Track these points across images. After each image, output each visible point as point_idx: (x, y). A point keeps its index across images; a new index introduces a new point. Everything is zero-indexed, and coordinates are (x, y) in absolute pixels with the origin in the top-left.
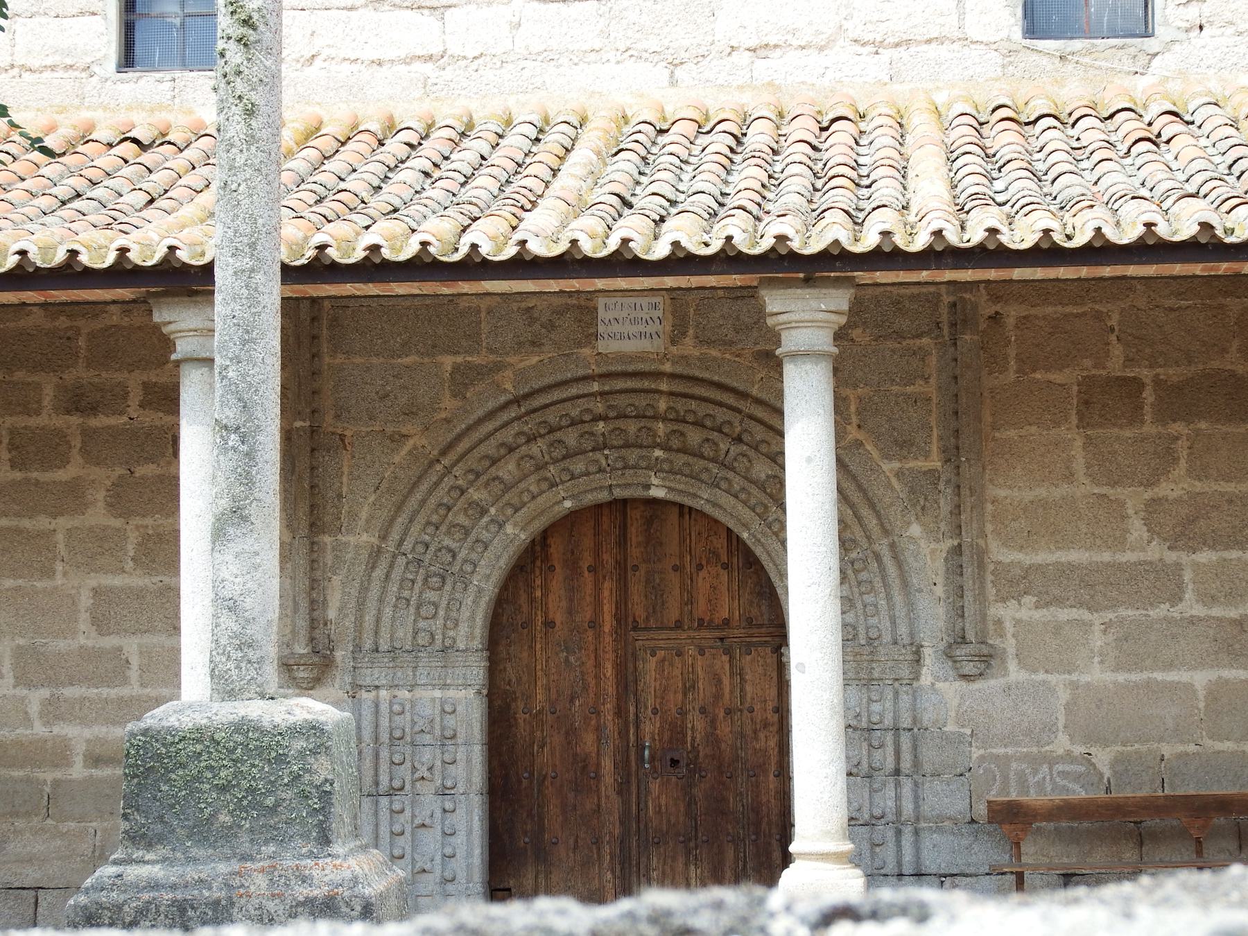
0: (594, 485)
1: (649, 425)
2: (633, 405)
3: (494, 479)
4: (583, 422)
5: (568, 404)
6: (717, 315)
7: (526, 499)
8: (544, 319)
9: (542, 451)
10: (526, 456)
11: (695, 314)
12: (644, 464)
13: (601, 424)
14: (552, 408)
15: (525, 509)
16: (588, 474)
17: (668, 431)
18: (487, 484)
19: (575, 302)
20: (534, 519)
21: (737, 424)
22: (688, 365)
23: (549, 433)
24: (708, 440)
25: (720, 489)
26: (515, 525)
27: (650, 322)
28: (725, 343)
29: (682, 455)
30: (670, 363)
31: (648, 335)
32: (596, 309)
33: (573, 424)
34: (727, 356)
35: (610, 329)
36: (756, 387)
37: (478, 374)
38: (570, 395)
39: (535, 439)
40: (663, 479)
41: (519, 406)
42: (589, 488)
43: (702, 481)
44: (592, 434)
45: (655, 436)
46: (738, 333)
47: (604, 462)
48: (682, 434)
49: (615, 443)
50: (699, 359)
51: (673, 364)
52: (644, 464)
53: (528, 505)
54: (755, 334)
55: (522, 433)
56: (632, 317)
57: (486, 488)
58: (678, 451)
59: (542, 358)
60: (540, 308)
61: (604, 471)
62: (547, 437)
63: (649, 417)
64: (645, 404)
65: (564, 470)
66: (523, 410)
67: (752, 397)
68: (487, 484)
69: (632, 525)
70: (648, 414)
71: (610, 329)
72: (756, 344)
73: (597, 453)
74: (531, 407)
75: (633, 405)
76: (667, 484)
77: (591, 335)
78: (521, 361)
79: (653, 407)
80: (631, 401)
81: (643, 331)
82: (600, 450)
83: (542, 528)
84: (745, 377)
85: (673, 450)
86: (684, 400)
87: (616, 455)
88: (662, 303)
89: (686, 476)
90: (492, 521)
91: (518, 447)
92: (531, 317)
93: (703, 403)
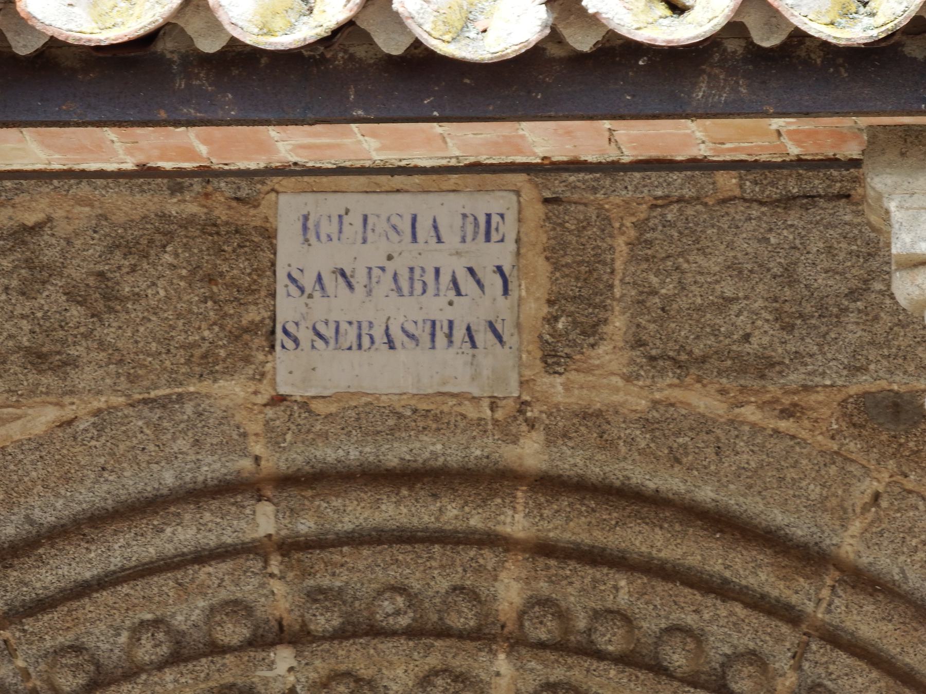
1: (459, 663)
2: (401, 590)
4: (216, 649)
5: (164, 583)
6: (713, 264)
8: (77, 271)
11: (633, 258)
14: (105, 596)
19: (192, 208)
21: (782, 662)
22: (607, 444)
27: (468, 283)
28: (741, 366)
31: (459, 333)
32: (269, 235)
34: (750, 413)
35: (320, 309)
36: (856, 527)
38: (169, 549)
46: (789, 328)
50: (646, 424)
51: (549, 442)
54: (853, 332)
56: (400, 265)
60: (63, 229)
63: (462, 635)
64: (444, 585)
67: (840, 565)
70: (455, 621)
71: (320, 309)
72: (855, 370)
74: (28, 594)
75: (401, 590)
77: (252, 329)
79: (474, 596)
80: (393, 575)
81: (442, 318)
84: (815, 491)
86: (590, 572)
88: (511, 216)
92: (29, 264)
93: (661, 587)
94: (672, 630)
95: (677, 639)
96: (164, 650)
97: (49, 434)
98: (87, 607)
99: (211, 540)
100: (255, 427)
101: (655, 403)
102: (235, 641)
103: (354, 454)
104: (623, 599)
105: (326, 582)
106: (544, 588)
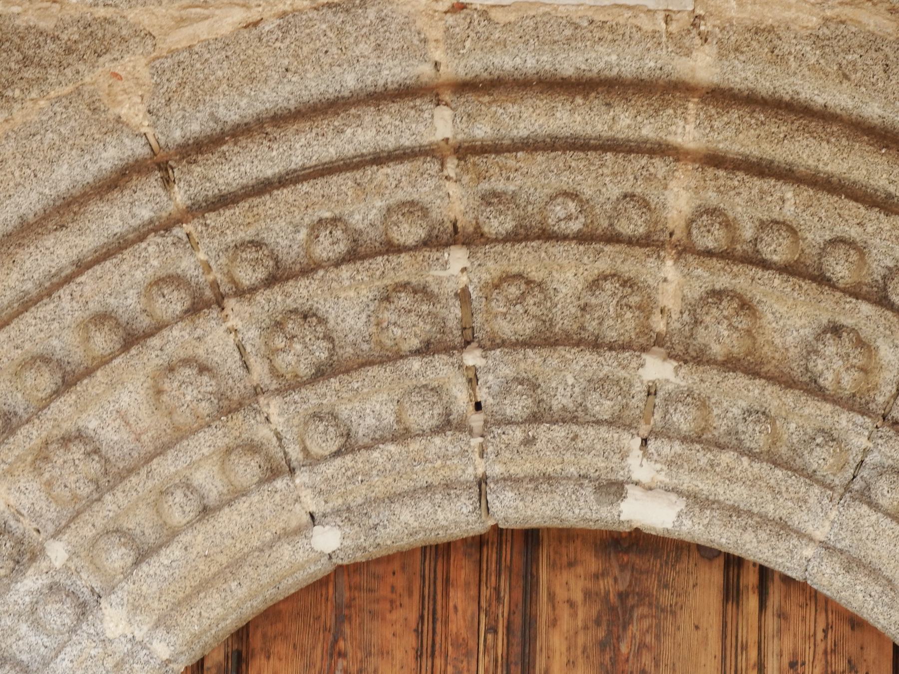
0: (423, 477)
1: (628, 268)
2: (573, 195)
3: (66, 441)
4: (391, 248)
5: (343, 182)
7: (177, 518)
9: (240, 348)
10: (186, 362)
12: (604, 407)
13: (457, 257)
14: (285, 194)
15: (174, 552)
16: (402, 435)
17: (696, 291)
18: (42, 456)
20: (204, 586)
22: (777, 58)
23: (271, 281)
24: (836, 330)
25: (874, 505)
26: (136, 608)
29: (740, 380)
30: (711, 49)
33: (353, 256)
37: (26, 61)
38: (349, 150)
39: (219, 301)
40: (672, 463)
41: (167, 182)
42: (404, 485)
43: (811, 477)
44: (423, 292)
45: (645, 309)
47: (461, 398)
48: (746, 306)
49: (505, 329)
50: (816, 40)
51: (721, 56)
52: (604, 407)
53: (185, 538)
55: (175, 280)
57: (37, 471)
58: (730, 364)
59: (254, 15)
61: (462, 427)
62: (260, 297)
63: (631, 242)
64: (615, 192)
65: (317, 416)
66: (180, 197)
68: (42, 456)
69: (554, 623)
70: (625, 228)
73: (440, 360)
74: (211, 190)
75: (573, 195)
76: (687, 481)
78: (181, 22)
79: (644, 204)
80: (566, 181)
82: (448, 349)
83: (231, 623)
85: (711, 362)
87: (507, 371)
89: (753, 455)
90: (53, 588)
91: (158, 328)
93: (826, 199)
94: (836, 242)
95: (841, 251)
96: (342, 247)
97: (236, 33)
98: (267, 203)
99: (389, 142)
100: (435, 33)
101: (826, 20)
102: (411, 241)
103: (531, 63)
104: (789, 211)
105: (500, 186)
106: (712, 198)
